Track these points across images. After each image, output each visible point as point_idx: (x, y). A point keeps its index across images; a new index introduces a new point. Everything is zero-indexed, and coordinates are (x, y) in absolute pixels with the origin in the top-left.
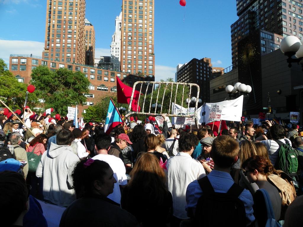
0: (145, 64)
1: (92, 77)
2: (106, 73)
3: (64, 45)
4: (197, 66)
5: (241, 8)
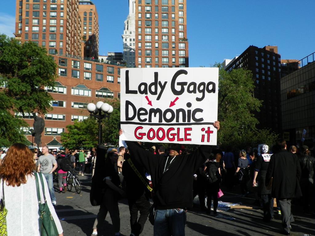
0: (173, 55)
1: (88, 75)
2: (110, 69)
3: (44, 28)
4: (257, 58)
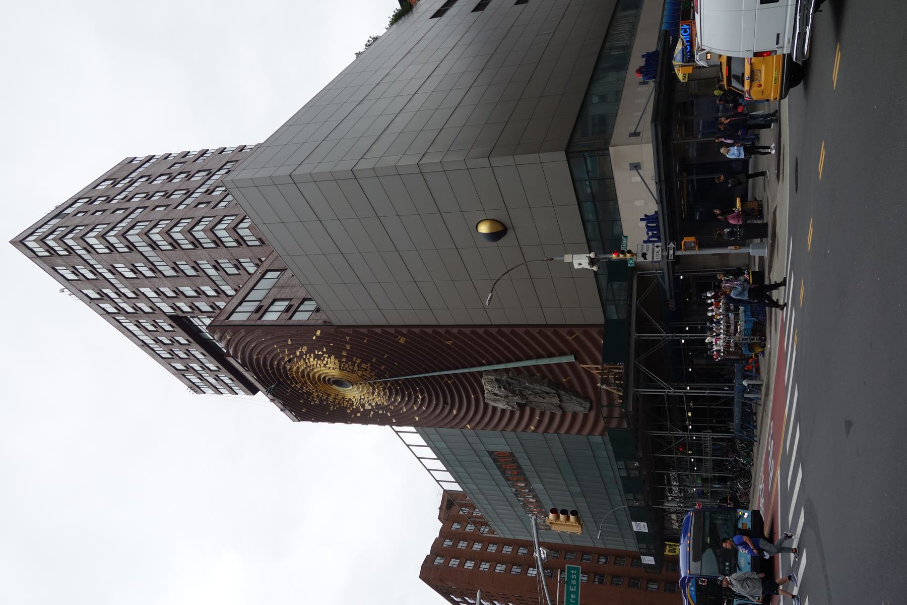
5: (228, 381)
